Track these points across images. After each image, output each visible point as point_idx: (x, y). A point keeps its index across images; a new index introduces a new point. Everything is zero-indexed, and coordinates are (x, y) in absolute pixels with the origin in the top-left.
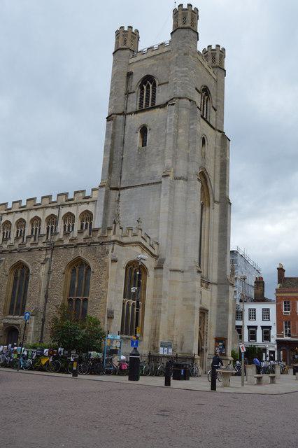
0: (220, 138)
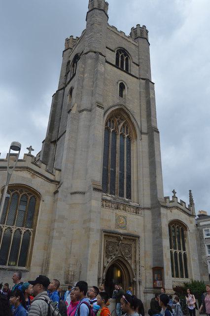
0: (144, 84)
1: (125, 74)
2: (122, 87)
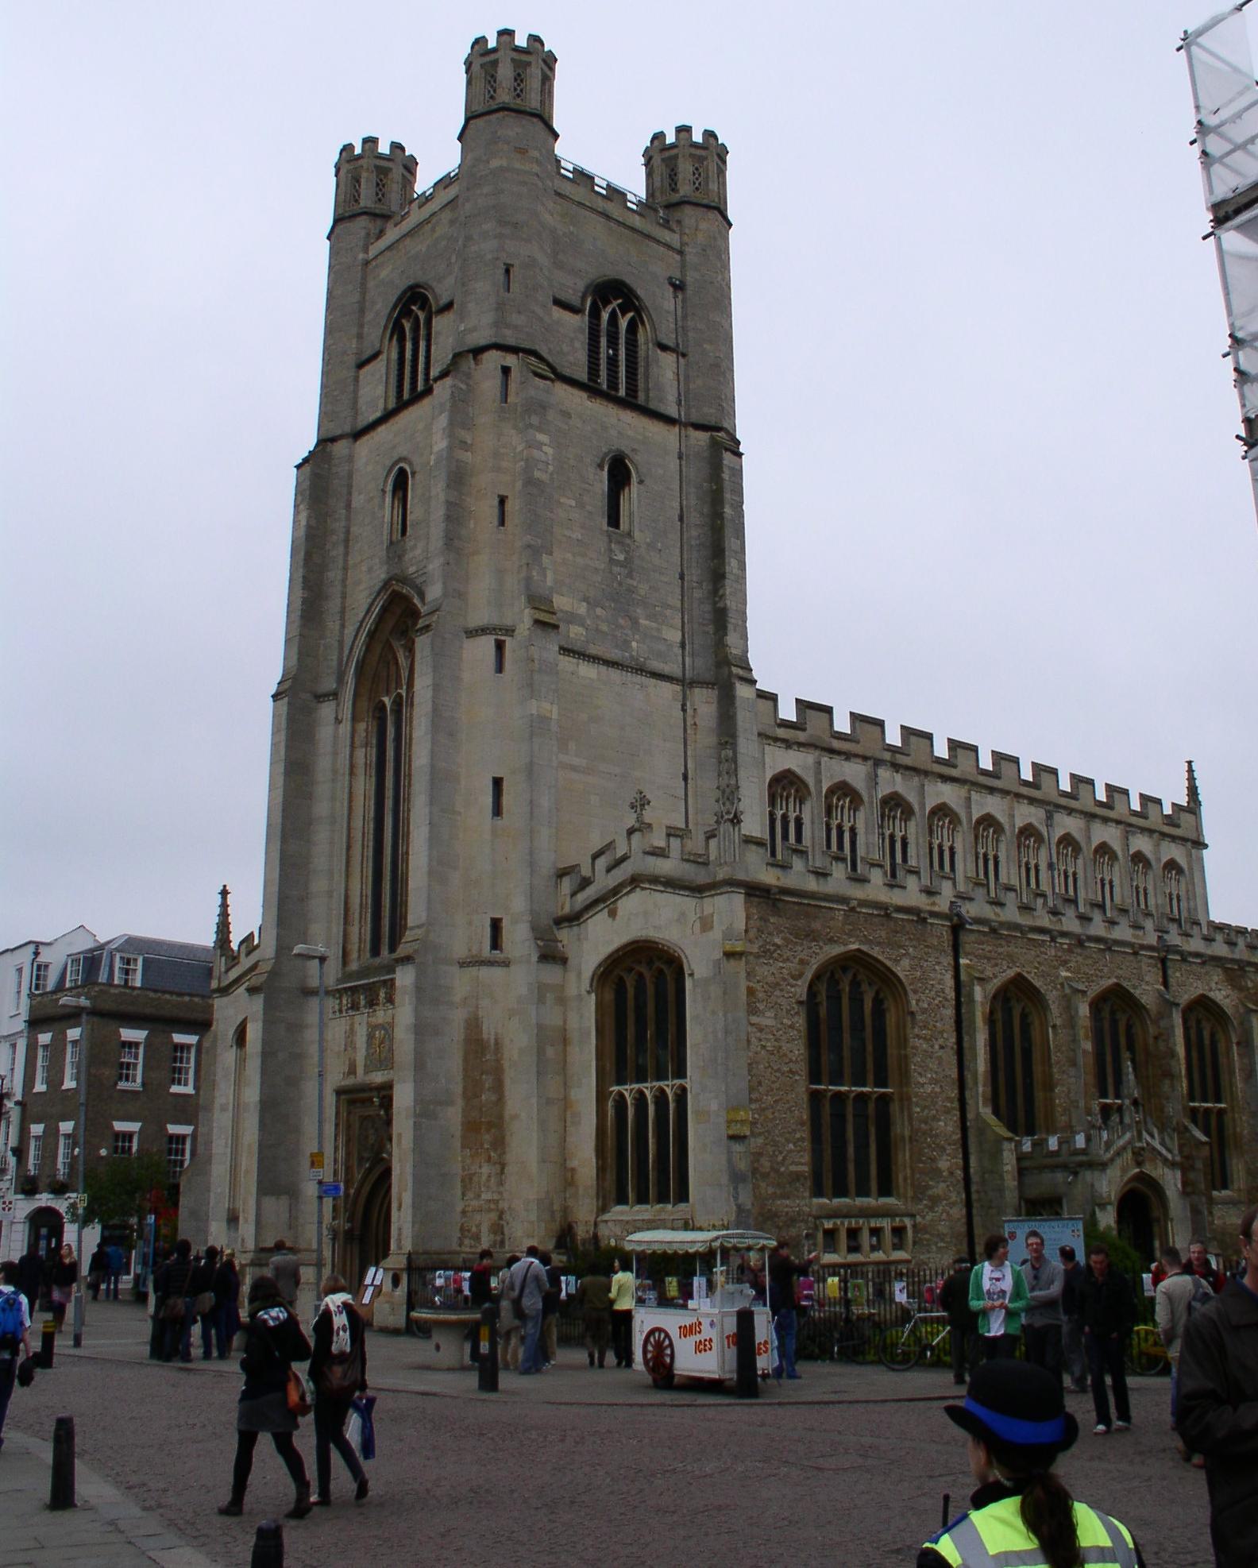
1: (628, 417)
2: (619, 472)
